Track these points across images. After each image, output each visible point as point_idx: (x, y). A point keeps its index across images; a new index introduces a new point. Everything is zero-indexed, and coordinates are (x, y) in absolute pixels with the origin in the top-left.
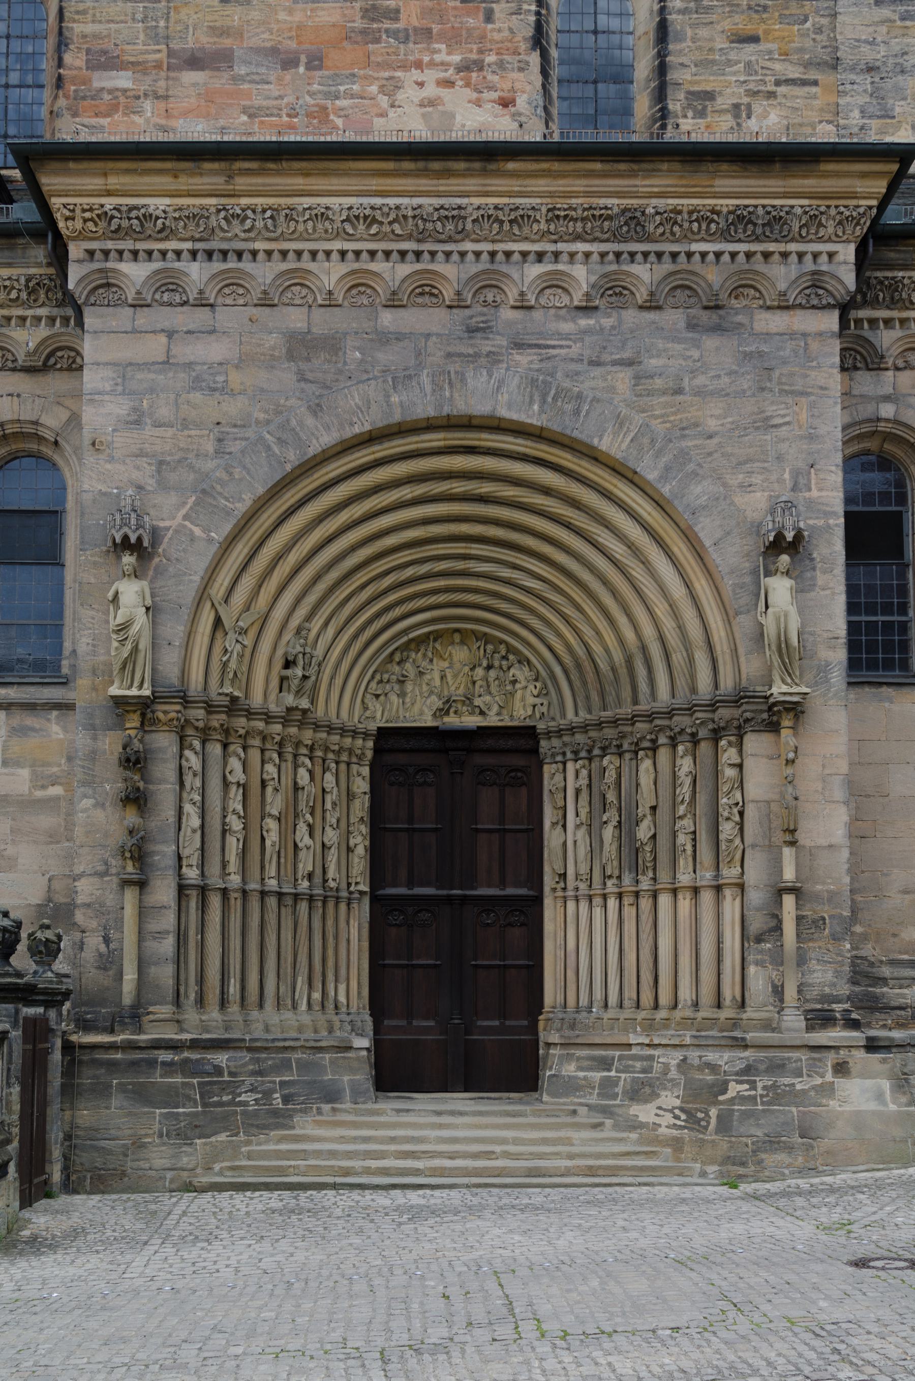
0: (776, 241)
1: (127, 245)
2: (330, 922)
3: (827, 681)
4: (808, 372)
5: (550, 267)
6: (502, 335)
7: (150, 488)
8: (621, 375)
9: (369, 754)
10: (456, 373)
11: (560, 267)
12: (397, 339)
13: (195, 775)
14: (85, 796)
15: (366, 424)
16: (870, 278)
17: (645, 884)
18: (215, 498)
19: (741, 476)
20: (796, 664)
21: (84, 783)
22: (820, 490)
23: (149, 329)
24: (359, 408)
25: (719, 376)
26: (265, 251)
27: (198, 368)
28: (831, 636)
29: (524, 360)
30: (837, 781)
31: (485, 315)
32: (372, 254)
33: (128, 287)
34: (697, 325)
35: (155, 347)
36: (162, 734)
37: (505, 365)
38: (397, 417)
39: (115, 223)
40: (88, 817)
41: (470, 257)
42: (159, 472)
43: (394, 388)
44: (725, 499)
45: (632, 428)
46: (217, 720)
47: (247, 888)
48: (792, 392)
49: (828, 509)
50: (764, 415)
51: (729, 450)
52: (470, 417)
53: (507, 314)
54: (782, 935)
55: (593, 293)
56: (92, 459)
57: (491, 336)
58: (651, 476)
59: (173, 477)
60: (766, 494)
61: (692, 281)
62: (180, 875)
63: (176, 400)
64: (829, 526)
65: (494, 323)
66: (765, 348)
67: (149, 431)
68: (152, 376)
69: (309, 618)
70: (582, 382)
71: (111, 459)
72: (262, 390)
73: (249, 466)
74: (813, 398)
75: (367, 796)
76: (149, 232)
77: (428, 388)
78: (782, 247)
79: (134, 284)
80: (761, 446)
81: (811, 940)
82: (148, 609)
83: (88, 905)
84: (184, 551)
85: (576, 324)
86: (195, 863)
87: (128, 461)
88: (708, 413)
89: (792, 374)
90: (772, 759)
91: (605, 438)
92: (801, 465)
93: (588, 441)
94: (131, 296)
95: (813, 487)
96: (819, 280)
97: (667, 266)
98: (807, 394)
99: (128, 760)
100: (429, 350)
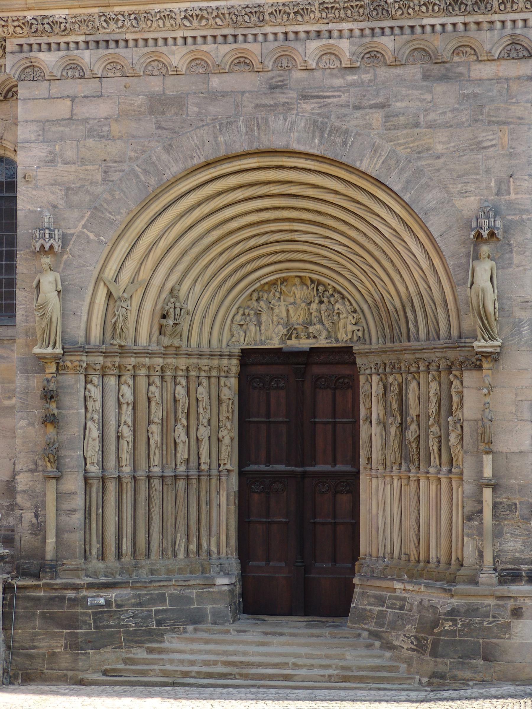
1: (43, 40)
2: (203, 494)
3: (520, 333)
4: (510, 107)
5: (324, 42)
6: (294, 90)
7: (61, 207)
8: (375, 116)
10: (262, 118)
12: (223, 96)
14: (22, 418)
15: (202, 157)
18: (103, 213)
19: (460, 186)
22: (517, 193)
25: (445, 113)
27: (91, 122)
28: (523, 300)
29: (308, 107)
31: (281, 76)
34: (430, 76)
36: (70, 376)
37: (295, 112)
38: (222, 153)
39: (34, 27)
40: (24, 432)
42: (66, 195)
43: (221, 131)
44: (448, 203)
49: (522, 207)
50: (477, 140)
53: (297, 75)
55: (354, 58)
57: (286, 91)
60: (478, 198)
62: (85, 470)
64: (523, 220)
65: (288, 82)
66: (478, 90)
67: (60, 167)
68: (62, 129)
70: (349, 122)
71: (36, 187)
72: (134, 137)
73: (125, 189)
74: (512, 126)
76: (56, 31)
77: (243, 129)
78: (488, 18)
80: (474, 163)
81: (506, 519)
82: (59, 292)
83: (24, 492)
84: (83, 249)
85: (344, 79)
86: (95, 461)
87: (46, 188)
88: (437, 140)
89: (498, 109)
91: (364, 161)
92: (503, 176)
95: (512, 192)
96: (516, 40)
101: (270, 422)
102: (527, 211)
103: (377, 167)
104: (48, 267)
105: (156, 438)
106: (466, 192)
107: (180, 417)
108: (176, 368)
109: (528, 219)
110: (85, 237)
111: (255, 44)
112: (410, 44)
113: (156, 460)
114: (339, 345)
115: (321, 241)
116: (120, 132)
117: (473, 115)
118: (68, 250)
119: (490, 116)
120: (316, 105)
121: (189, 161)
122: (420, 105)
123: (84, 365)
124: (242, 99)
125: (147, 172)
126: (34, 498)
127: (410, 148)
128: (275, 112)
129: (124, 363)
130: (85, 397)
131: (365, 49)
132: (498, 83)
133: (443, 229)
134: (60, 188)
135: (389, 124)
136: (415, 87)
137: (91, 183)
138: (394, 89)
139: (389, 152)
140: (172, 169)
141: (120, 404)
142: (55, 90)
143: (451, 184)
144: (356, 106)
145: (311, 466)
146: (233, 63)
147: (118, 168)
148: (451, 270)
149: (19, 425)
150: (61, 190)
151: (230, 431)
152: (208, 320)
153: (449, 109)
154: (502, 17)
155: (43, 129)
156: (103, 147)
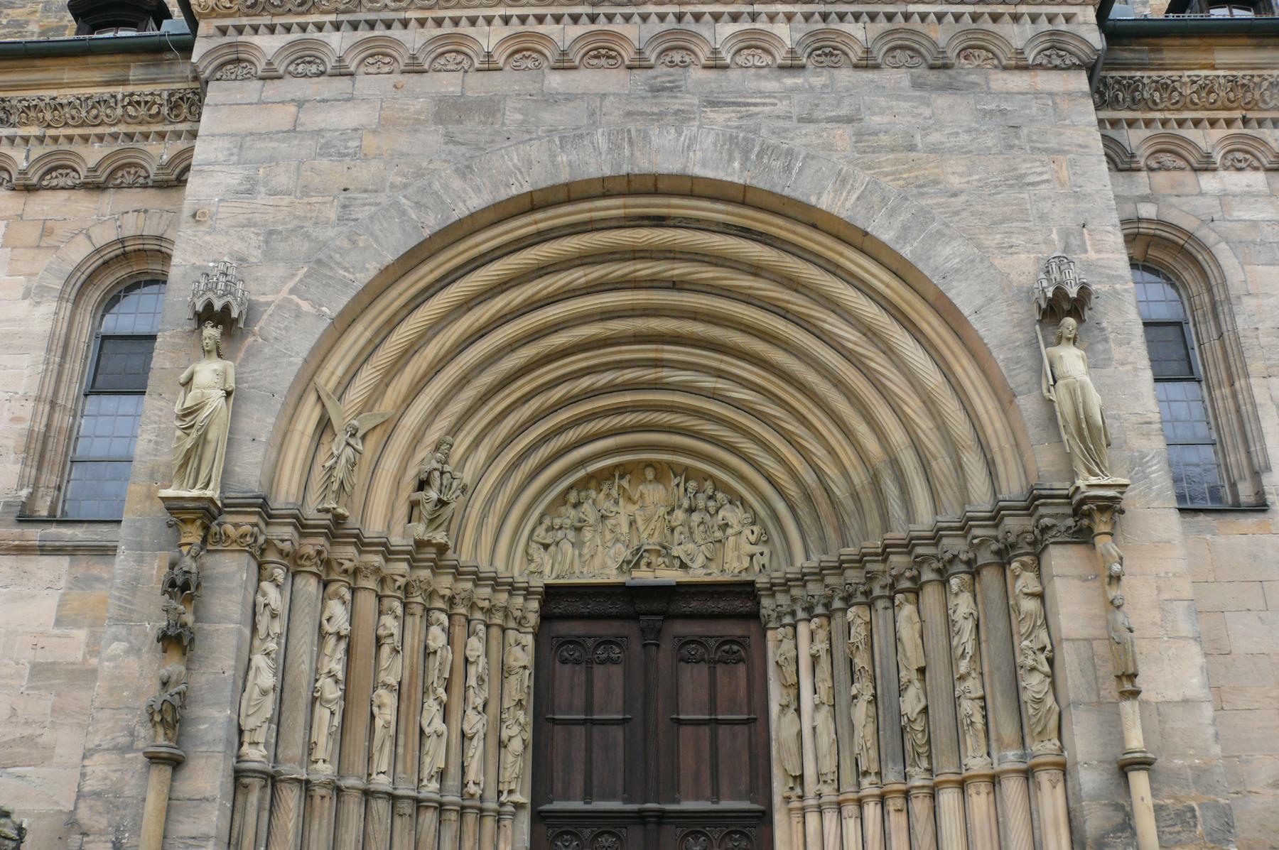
3: (1146, 477)
7: (253, 260)
8: (840, 132)
9: (533, 619)
10: (638, 131)
11: (758, 26)
13: (274, 616)
14: (116, 638)
18: (331, 269)
19: (998, 236)
20: (1105, 451)
21: (117, 621)
22: (1099, 251)
23: (278, 99)
24: (519, 169)
25: (957, 134)
27: (328, 135)
29: (720, 117)
30: (1180, 609)
32: (540, 19)
33: (258, 60)
35: (282, 117)
36: (229, 555)
38: (564, 177)
40: (116, 667)
41: (654, 18)
42: (267, 242)
43: (562, 147)
44: (982, 261)
45: (857, 185)
46: (310, 546)
47: (343, 783)
48: (1046, 150)
51: (980, 208)
52: (657, 177)
53: (696, 74)
54: (1134, 834)
55: (799, 51)
56: (189, 232)
57: (679, 95)
58: (886, 236)
59: (282, 248)
63: (298, 168)
64: (1116, 292)
66: (1004, 106)
67: (261, 199)
69: (455, 429)
70: (792, 139)
71: (212, 230)
72: (402, 154)
73: (378, 233)
74: (1071, 156)
75: (527, 672)
82: (228, 394)
83: (97, 795)
86: (262, 740)
87: (232, 231)
88: (949, 170)
90: (1086, 580)
93: (804, 199)
94: (261, 67)
95: (1089, 248)
96: (1059, 41)
97: (882, 25)
98: (1066, 152)
99: (172, 584)
100: (604, 110)
101: (593, 722)
103: (848, 205)
104: (215, 347)
105: (386, 716)
106: (1011, 247)
107: (435, 685)
108: (431, 595)
110: (293, 307)
111: (628, 26)
112: (890, 38)
113: (382, 762)
115: (708, 382)
116: (378, 148)
117: (1004, 139)
119: (1032, 141)
121: (503, 191)
122: (913, 121)
123: (261, 539)
124: (601, 103)
125: (421, 206)
126: (117, 807)
130: (255, 605)
132: (1036, 98)
133: (978, 301)
134: (256, 231)
136: (899, 97)
137: (316, 223)
138: (866, 98)
139: (867, 184)
140: (468, 203)
141: (322, 635)
143: (981, 234)
146: (588, 56)
147: (368, 201)
148: (1003, 369)
149: (109, 651)
150: (257, 234)
151: (523, 729)
152: (492, 521)
153: (963, 129)
155: (241, 146)
156: (345, 169)
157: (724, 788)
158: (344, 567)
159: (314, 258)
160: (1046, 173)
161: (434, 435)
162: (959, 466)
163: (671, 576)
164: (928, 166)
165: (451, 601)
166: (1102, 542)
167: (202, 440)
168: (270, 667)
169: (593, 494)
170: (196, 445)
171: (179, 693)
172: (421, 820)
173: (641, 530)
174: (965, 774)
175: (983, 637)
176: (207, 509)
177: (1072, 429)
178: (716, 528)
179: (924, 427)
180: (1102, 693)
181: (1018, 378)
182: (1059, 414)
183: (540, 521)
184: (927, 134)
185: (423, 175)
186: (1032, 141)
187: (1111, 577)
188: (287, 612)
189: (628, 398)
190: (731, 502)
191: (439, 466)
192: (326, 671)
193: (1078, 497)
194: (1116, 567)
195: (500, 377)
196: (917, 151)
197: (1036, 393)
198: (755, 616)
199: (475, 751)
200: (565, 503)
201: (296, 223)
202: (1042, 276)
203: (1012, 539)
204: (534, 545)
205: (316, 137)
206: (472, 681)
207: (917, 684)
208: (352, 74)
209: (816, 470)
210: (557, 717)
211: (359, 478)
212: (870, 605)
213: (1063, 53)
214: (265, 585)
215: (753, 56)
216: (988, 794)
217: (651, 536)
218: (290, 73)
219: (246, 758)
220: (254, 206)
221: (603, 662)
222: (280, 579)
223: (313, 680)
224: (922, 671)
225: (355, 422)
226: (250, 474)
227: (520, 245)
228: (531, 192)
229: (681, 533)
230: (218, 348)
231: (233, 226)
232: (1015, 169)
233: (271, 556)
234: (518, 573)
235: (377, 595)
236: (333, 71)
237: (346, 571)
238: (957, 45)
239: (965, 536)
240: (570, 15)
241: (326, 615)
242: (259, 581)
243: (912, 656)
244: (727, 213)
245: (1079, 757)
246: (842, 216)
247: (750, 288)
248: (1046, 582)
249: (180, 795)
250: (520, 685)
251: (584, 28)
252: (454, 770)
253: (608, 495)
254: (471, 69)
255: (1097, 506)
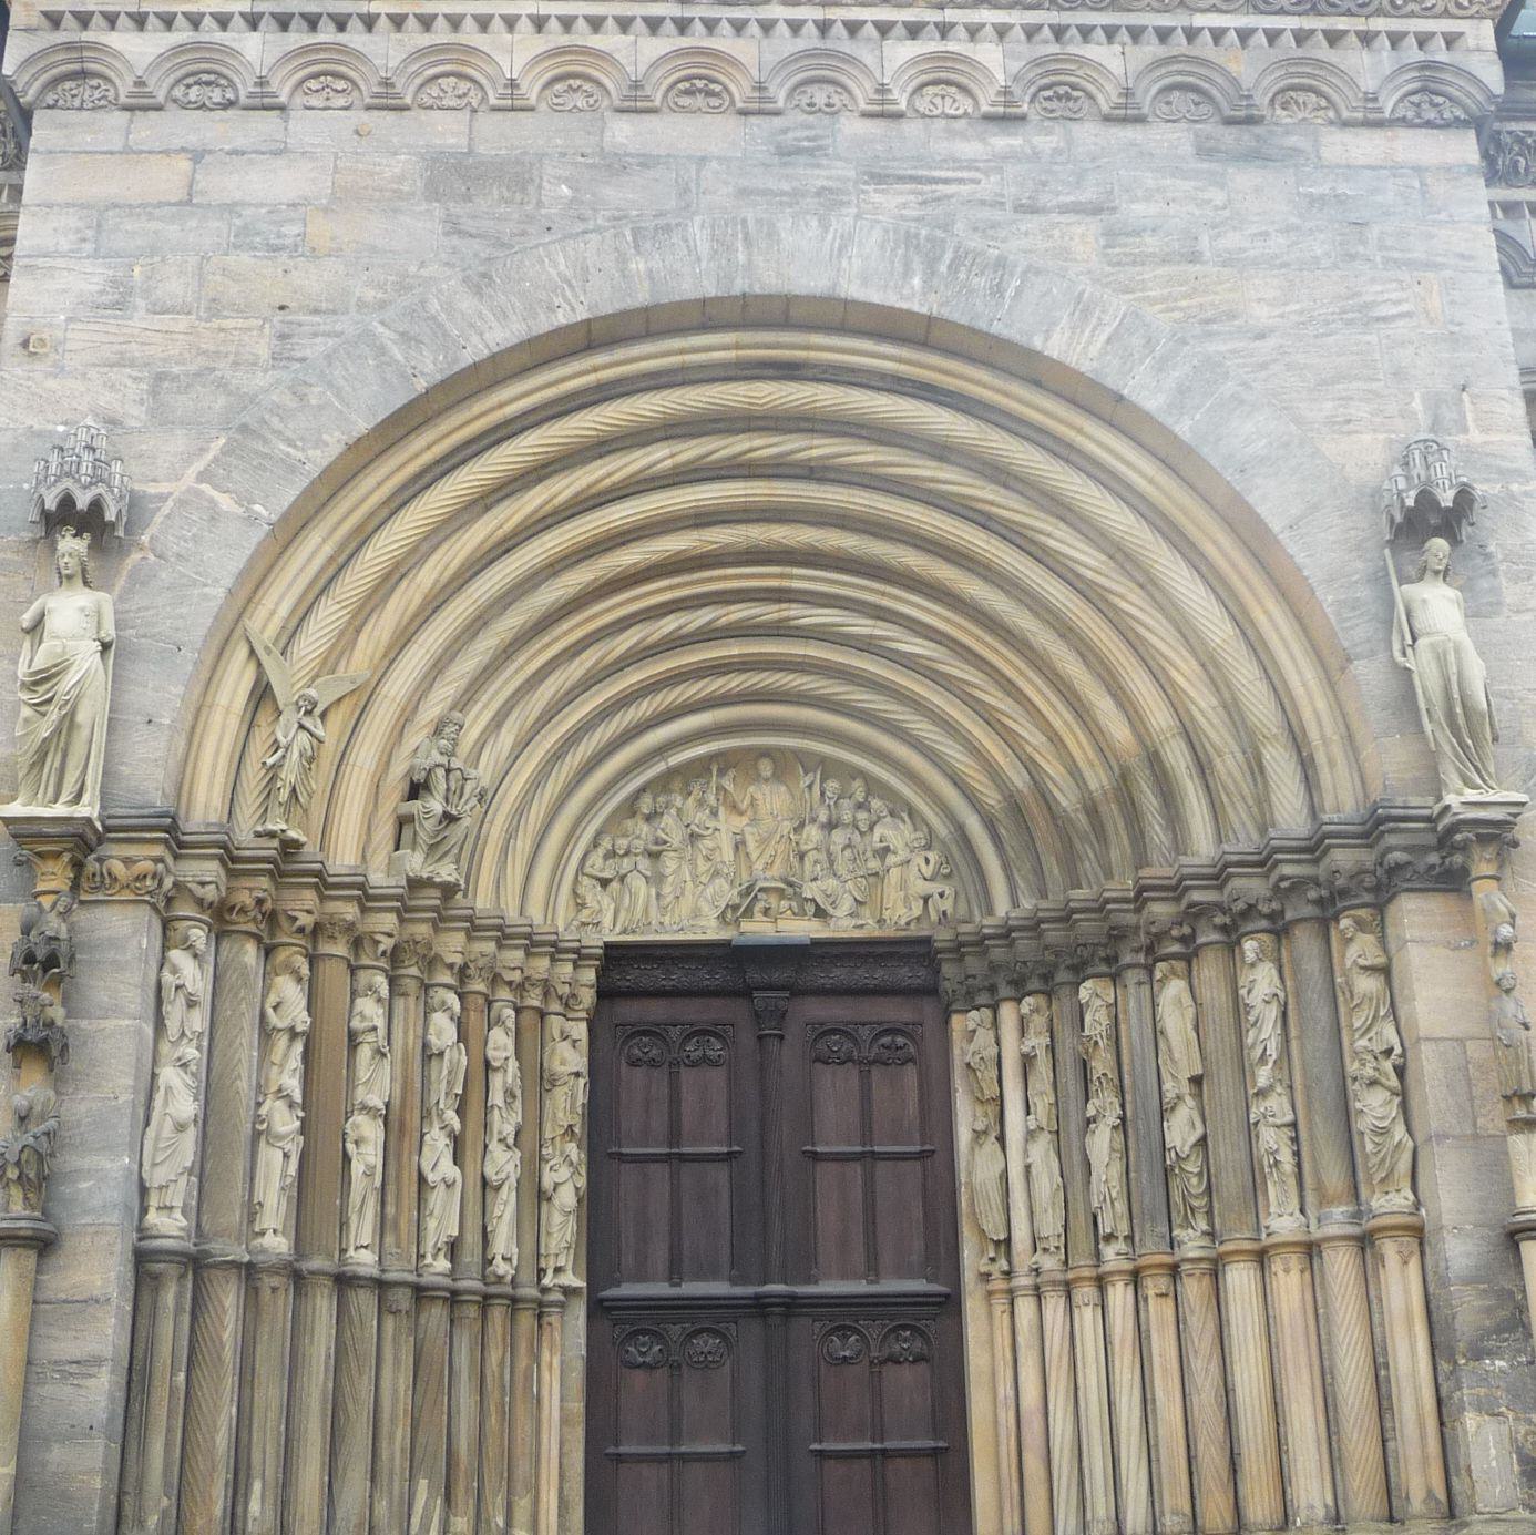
0: (1349, 13)
6: (846, 160)
7: (133, 423)
8: (1079, 230)
9: (588, 997)
10: (759, 221)
11: (951, 46)
12: (641, 165)
15: (580, 308)
16: (1499, 133)
17: (1192, 1243)
18: (266, 441)
19: (1329, 405)
20: (1490, 748)
23: (157, 146)
25: (1266, 235)
26: (389, 16)
27: (247, 212)
29: (891, 201)
31: (810, 127)
33: (121, 76)
35: (167, 178)
36: (117, 908)
37: (853, 210)
38: (642, 297)
41: (782, 29)
42: (154, 393)
43: (637, 247)
45: (1107, 318)
47: (305, 1266)
48: (1409, 263)
49: (1508, 465)
52: (789, 300)
53: (853, 127)
55: (1017, 90)
56: (19, 371)
57: (824, 162)
61: (1201, 77)
62: (140, 1229)
64: (1512, 497)
65: (829, 141)
66: (1343, 188)
67: (139, 320)
68: (154, 225)
69: (465, 700)
71: (59, 371)
72: (373, 249)
73: (342, 382)
74: (1447, 273)
75: (582, 1082)
77: (704, 247)
78: (1359, 24)
79: (130, 68)
82: (106, 647)
86: (178, 1203)
90: (1458, 948)
91: (1056, 336)
94: (124, 89)
95: (1470, 424)
97: (1151, 49)
98: (1437, 267)
99: (30, 958)
101: (683, 1158)
102: (1518, 473)
103: (1094, 351)
106: (1349, 421)
107: (441, 1106)
109: (1526, 494)
110: (206, 504)
111: (741, 42)
112: (1163, 70)
113: (363, 1228)
114: (889, 932)
115: (862, 626)
118: (145, 538)
119: (1387, 248)
120: (912, 197)
121: (542, 317)
122: (1197, 212)
123: (168, 882)
125: (410, 339)
127: (1181, 309)
128: (797, 208)
129: (290, 905)
131: (1041, 76)
134: (135, 374)
135: (1117, 250)
140: (487, 336)
141: (266, 1033)
142: (143, 134)
144: (1022, 206)
145: (810, 1280)
146: (675, 91)
147: (322, 328)
148: (1333, 618)
152: (523, 844)
154: (1395, 24)
155: (99, 225)
157: (887, 1257)
158: (298, 923)
159: (237, 423)
160: (1407, 300)
161: (432, 709)
162: (1256, 767)
163: (801, 929)
164: (1219, 288)
165: (463, 973)
166: (1482, 891)
167: (68, 723)
168: (187, 1086)
169: (678, 801)
170: (57, 732)
171: (47, 1134)
172: (423, 1321)
173: (754, 857)
174: (1266, 1241)
175: (1293, 1032)
176: (81, 837)
177: (1440, 714)
178: (869, 854)
179: (1203, 705)
180: (1480, 1121)
181: (1357, 632)
182: (1419, 691)
183: (595, 844)
184: (1218, 235)
185: (411, 288)
186: (1387, 248)
187: (1496, 945)
188: (209, 997)
189: (734, 649)
190: (892, 814)
191: (443, 760)
192: (275, 1088)
193: (1447, 821)
194: (1506, 931)
195: (536, 615)
196: (1203, 263)
197: (1382, 656)
198: (931, 991)
199: (505, 1207)
200: (633, 814)
201: (202, 361)
202: (1398, 470)
203: (1340, 882)
204: (586, 881)
205: (226, 215)
206: (497, 1097)
207: (1190, 1101)
208: (282, 108)
209: (1030, 765)
210: (624, 1150)
211: (319, 782)
212: (1115, 978)
213: (1440, 100)
214: (176, 955)
215: (943, 97)
216: (1302, 1272)
217: (769, 865)
218: (175, 101)
219: (155, 1232)
220: (128, 331)
221: (694, 1065)
222: (201, 945)
223: (252, 1103)
224: (1196, 1081)
225: (312, 692)
226: (147, 781)
227: (568, 406)
228: (588, 321)
229: (816, 862)
230: (84, 571)
231: (94, 365)
232: (1358, 294)
233: (185, 909)
234: (563, 922)
235: (349, 966)
236: (250, 101)
237: (301, 930)
238: (1272, 83)
239: (1266, 876)
240: (646, 19)
241: (272, 999)
242: (165, 948)
243: (1182, 1058)
244: (900, 360)
245: (1446, 1219)
246: (1082, 370)
247: (932, 480)
248: (1392, 946)
249: (50, 1295)
250: (567, 1103)
251: (667, 42)
252: (472, 1239)
253: (701, 803)
254: (483, 107)
255: (1477, 835)
